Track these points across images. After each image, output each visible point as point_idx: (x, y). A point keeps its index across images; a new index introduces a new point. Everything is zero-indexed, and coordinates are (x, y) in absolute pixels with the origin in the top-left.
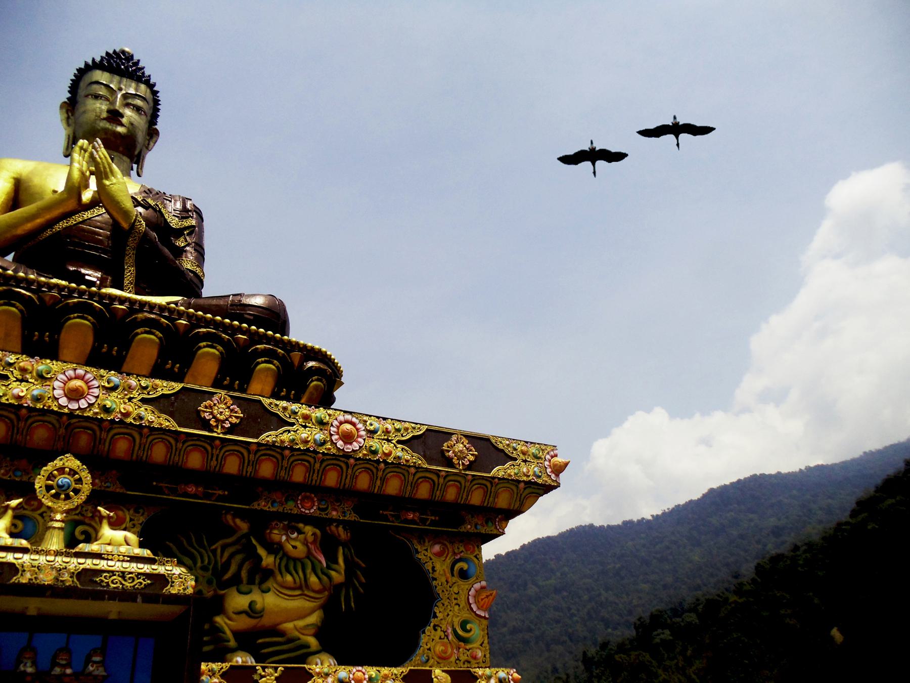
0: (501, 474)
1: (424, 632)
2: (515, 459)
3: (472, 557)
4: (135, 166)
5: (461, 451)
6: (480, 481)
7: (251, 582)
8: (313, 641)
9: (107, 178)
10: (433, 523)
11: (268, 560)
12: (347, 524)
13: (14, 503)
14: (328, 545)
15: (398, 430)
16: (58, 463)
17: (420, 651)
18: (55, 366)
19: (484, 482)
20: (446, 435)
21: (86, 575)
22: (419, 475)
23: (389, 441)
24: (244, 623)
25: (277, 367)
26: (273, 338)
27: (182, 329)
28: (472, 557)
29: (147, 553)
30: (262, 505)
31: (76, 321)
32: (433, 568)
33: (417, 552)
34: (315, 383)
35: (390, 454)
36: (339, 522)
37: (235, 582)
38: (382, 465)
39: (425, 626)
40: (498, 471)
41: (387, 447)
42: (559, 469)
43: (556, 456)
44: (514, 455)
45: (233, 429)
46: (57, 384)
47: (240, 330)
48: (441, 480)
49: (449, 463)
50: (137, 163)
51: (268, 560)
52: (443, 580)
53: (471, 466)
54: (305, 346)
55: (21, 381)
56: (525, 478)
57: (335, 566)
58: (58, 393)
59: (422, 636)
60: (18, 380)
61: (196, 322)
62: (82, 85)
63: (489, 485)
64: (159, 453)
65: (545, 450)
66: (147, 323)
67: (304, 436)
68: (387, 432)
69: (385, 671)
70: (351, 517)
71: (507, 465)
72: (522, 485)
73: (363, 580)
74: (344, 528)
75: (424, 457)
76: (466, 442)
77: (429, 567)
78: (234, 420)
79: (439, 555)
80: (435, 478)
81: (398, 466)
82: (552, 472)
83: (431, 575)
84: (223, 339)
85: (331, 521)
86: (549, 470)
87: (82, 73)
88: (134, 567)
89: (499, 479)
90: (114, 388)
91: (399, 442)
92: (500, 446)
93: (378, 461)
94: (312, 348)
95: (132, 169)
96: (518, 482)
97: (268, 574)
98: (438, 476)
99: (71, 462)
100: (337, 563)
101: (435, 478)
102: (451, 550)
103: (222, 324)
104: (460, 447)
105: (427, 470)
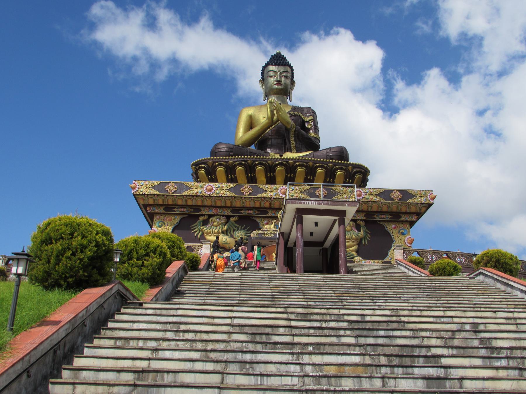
0: (411, 201)
1: (390, 251)
2: (417, 196)
3: (406, 228)
4: (288, 97)
5: (397, 196)
6: (404, 204)
8: (355, 253)
9: (280, 112)
10: (390, 218)
12: (363, 220)
13: (274, 221)
14: (358, 228)
15: (375, 191)
17: (388, 257)
18: (278, 186)
19: (405, 204)
20: (391, 191)
22: (382, 204)
23: (372, 195)
25: (344, 173)
26: (341, 163)
27: (311, 166)
28: (406, 228)
32: (392, 232)
33: (387, 227)
34: (357, 176)
35: (372, 198)
36: (361, 220)
38: (370, 202)
39: (390, 249)
40: (410, 201)
41: (371, 197)
42: (433, 198)
43: (432, 194)
44: (416, 195)
46: (279, 191)
48: (390, 205)
49: (392, 199)
50: (289, 96)
52: (396, 235)
53: (400, 200)
54: (353, 164)
55: (270, 191)
56: (420, 202)
57: (360, 233)
58: (279, 193)
59: (389, 252)
60: (269, 191)
61: (315, 162)
62: (265, 72)
63: (407, 205)
65: (426, 193)
66: (299, 165)
67: (345, 196)
68: (371, 192)
69: (376, 261)
71: (413, 199)
72: (419, 204)
73: (370, 236)
74: (362, 221)
75: (384, 198)
76: (398, 192)
77: (390, 232)
78: (325, 194)
79: (395, 228)
80: (388, 204)
81: (375, 202)
82: (430, 199)
83: (392, 235)
84: (324, 166)
85: (358, 220)
86: (429, 199)
87: (264, 68)
89: (411, 203)
90: (293, 190)
91: (375, 195)
92: (411, 193)
93: (369, 201)
94: (356, 164)
95: (288, 99)
96: (418, 203)
98: (389, 204)
100: (360, 231)
101: (388, 204)
102: (398, 226)
104: (396, 194)
105: (385, 202)
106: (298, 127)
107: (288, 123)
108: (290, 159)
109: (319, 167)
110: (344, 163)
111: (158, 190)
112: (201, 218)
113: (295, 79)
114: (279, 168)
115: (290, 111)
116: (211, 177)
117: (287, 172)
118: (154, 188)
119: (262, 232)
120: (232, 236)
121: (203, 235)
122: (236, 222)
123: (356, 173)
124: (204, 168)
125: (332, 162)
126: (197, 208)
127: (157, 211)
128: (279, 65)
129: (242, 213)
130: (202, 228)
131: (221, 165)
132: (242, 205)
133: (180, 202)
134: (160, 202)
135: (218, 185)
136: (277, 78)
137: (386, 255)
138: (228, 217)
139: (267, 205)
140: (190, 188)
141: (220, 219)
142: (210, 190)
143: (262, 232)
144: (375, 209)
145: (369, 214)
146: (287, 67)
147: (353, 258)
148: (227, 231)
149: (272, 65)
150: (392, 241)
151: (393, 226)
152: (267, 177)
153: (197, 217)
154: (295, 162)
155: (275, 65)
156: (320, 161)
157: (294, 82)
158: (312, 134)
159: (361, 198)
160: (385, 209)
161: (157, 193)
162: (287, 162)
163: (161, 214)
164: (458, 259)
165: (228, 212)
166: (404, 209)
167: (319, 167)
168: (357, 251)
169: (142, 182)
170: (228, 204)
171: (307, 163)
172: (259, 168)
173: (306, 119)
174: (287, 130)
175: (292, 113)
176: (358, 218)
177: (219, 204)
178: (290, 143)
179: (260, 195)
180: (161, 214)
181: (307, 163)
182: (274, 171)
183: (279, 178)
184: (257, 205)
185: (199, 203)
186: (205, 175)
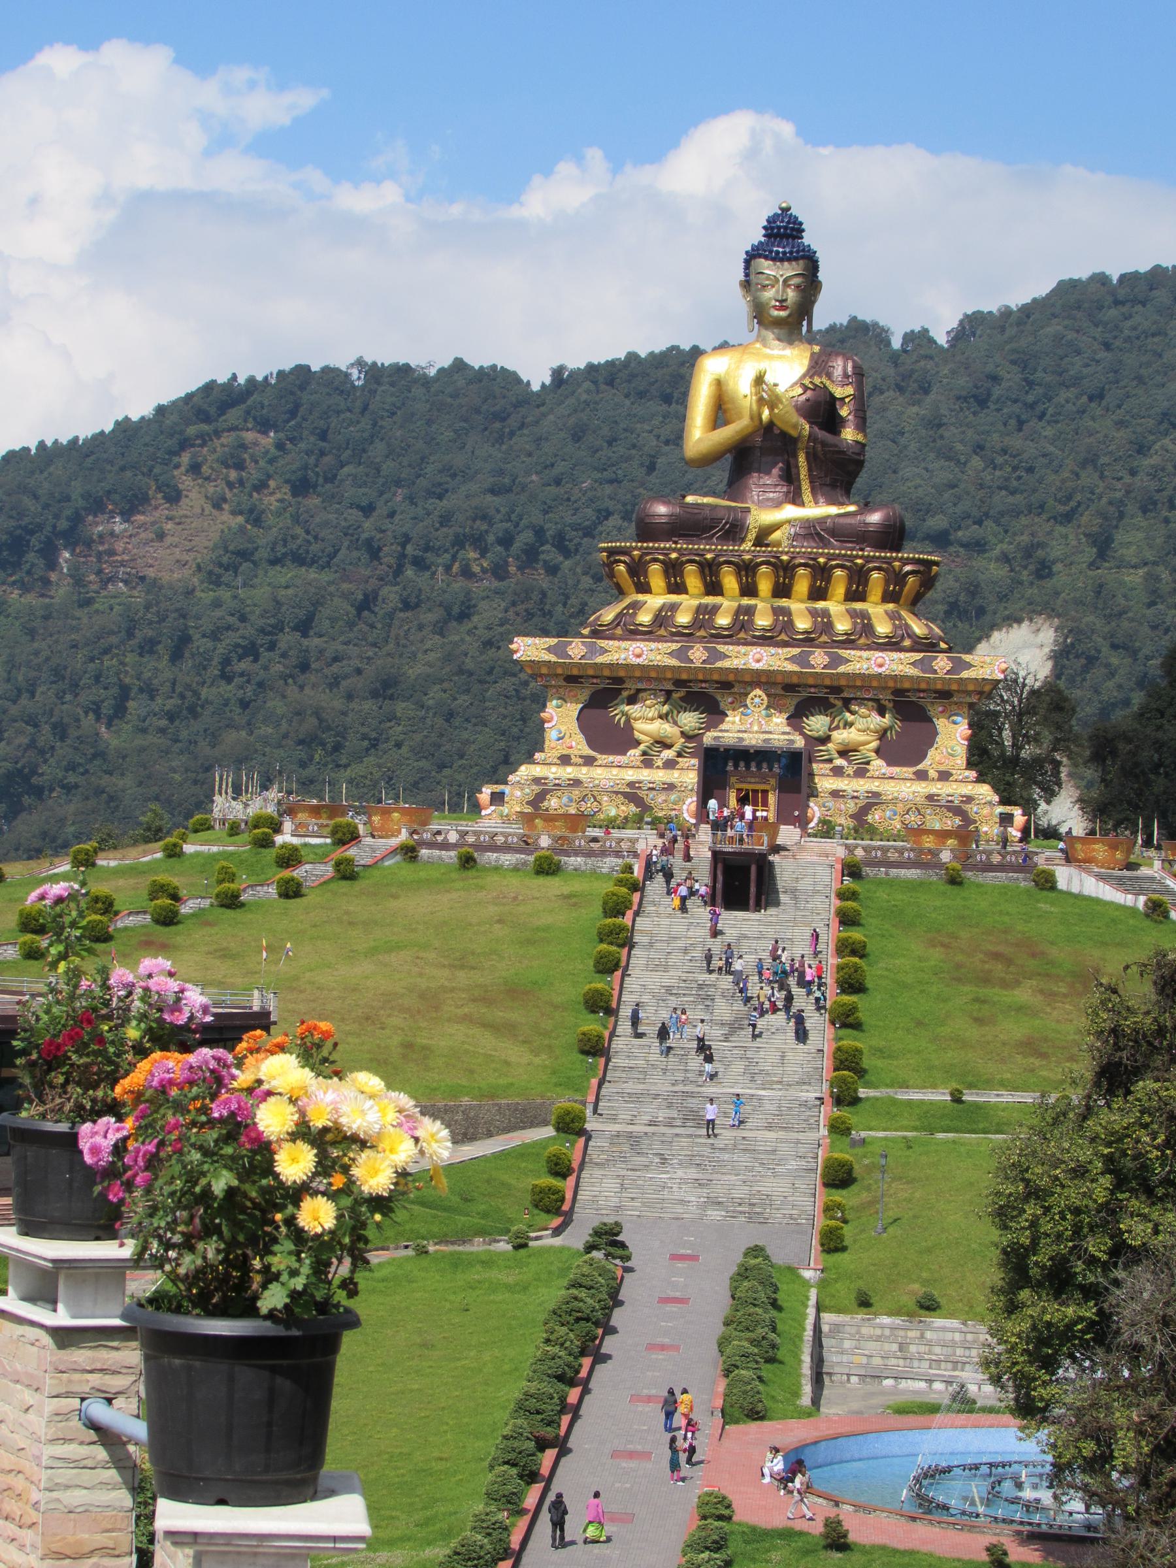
7: (844, 728)
8: (873, 754)
16: (754, 693)
21: (765, 741)
24: (841, 748)
29: (788, 729)
30: (845, 695)
37: (837, 728)
40: (965, 674)
41: (901, 667)
45: (825, 667)
47: (857, 557)
49: (935, 672)
53: (948, 672)
64: (795, 680)
69: (905, 769)
70: (892, 697)
88: (782, 737)
97: (851, 725)
99: (758, 692)
103: (845, 555)
104: (942, 663)
106: (816, 429)
107: (795, 426)
108: (782, 553)
109: (837, 566)
110: (885, 558)
111: (556, 654)
112: (625, 694)
113: (821, 276)
114: (763, 569)
115: (804, 376)
116: (639, 579)
117: (777, 576)
118: (549, 649)
119: (720, 734)
120: (675, 723)
121: (628, 721)
122: (681, 699)
123: (909, 573)
124: (624, 562)
125: (861, 557)
126: (619, 680)
128: (782, 260)
129: (690, 687)
130: (627, 708)
131: (655, 560)
132: (692, 677)
133: (591, 672)
134: (559, 671)
135: (653, 645)
136: (777, 291)
137: (925, 756)
140: (607, 651)
141: (655, 695)
142: (639, 656)
143: (720, 734)
144: (907, 685)
145: (898, 692)
146: (801, 262)
147: (868, 763)
148: (667, 715)
149: (766, 258)
150: (936, 733)
151: (940, 709)
152: (740, 582)
153: (619, 691)
154: (793, 558)
155: (773, 260)
156: (839, 555)
157: (820, 282)
158: (849, 434)
159: (883, 669)
160: (923, 686)
161: (553, 658)
162: (778, 558)
163: (560, 687)
164: (906, 855)
165: (670, 687)
166: (954, 687)
167: (837, 566)
168: (877, 751)
169: (529, 640)
170: (669, 675)
171: (814, 559)
172: (726, 569)
173: (838, 392)
175: (807, 382)
177: (653, 674)
178: (797, 467)
179: (719, 664)
180: (560, 687)
181: (814, 559)
182: (754, 574)
183: (765, 586)
184: (716, 677)
185: (622, 674)
186: (626, 575)
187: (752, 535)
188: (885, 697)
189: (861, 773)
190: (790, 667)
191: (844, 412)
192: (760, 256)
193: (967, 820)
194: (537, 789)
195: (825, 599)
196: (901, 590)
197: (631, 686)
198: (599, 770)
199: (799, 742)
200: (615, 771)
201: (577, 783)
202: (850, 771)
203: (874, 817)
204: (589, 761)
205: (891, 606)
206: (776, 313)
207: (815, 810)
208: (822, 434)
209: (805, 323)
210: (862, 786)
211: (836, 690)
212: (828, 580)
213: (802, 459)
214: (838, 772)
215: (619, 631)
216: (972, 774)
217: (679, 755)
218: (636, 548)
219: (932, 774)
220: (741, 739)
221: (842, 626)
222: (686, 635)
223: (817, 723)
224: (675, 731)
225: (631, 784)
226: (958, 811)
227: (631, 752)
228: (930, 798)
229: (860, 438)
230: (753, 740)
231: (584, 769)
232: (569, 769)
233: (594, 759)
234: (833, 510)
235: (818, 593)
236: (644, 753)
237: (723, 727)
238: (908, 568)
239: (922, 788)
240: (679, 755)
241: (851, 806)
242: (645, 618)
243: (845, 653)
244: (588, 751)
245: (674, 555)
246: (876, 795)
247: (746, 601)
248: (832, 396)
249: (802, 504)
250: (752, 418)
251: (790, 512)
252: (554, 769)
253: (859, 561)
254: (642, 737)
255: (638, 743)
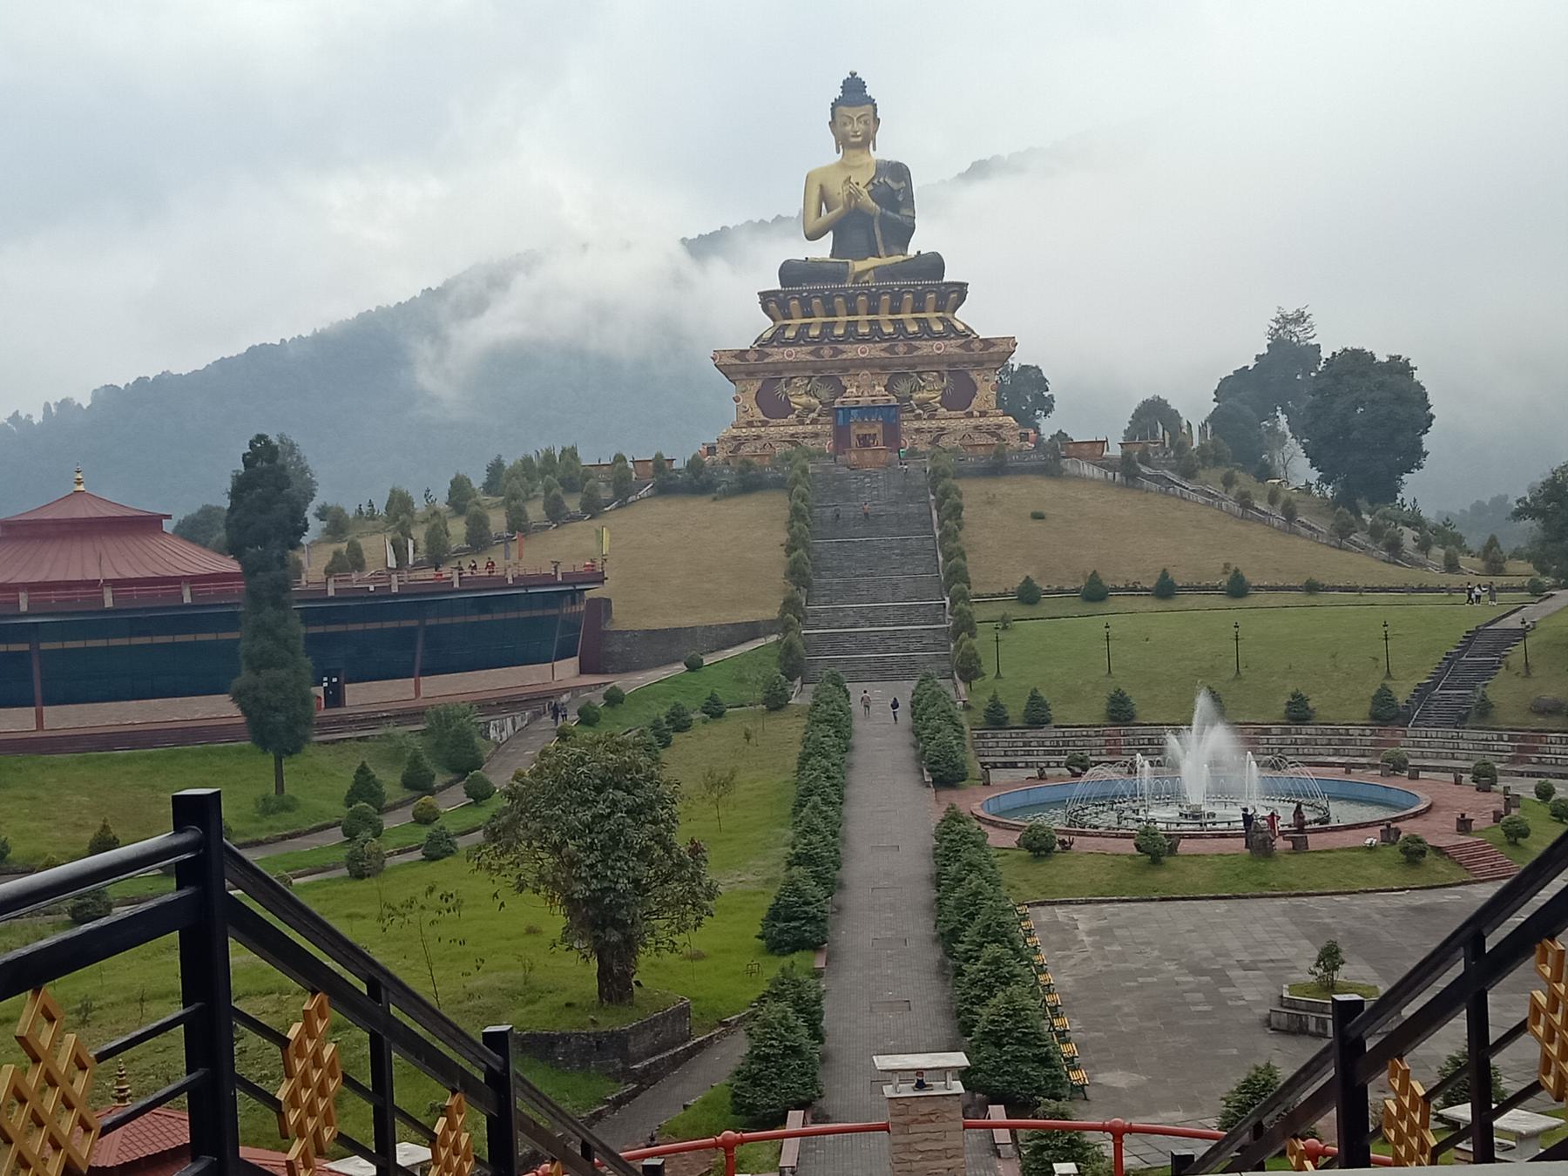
8: (938, 405)
11: (923, 384)
21: (873, 401)
31: (860, 298)
37: (915, 390)
49: (973, 350)
51: (923, 384)
81: (956, 354)
107: (871, 209)
108: (872, 287)
112: (783, 380)
113: (878, 116)
115: (873, 178)
121: (786, 398)
126: (780, 372)
127: (739, 377)
134: (742, 368)
138: (810, 378)
139: (848, 362)
144: (956, 359)
145: (950, 365)
152: (847, 307)
160: (966, 359)
173: (895, 186)
174: (872, 218)
175: (875, 182)
176: (940, 369)
183: (862, 308)
185: (780, 367)
187: (851, 278)
188: (943, 368)
189: (931, 417)
190: (883, 354)
191: (900, 199)
192: (840, 105)
193: (999, 437)
194: (735, 443)
195: (899, 313)
196: (946, 302)
197: (787, 375)
198: (772, 429)
199: (894, 402)
200: (782, 429)
201: (759, 437)
202: (926, 416)
203: (945, 442)
204: (764, 424)
205: (941, 314)
206: (853, 140)
207: (907, 442)
208: (890, 213)
209: (871, 145)
210: (934, 424)
211: (912, 366)
212: (901, 300)
213: (877, 231)
214: (918, 417)
215: (775, 344)
216: (1000, 411)
217: (819, 415)
218: (781, 291)
219: (975, 413)
220: (858, 402)
221: (912, 328)
222: (817, 342)
223: (903, 387)
224: (816, 401)
225: (792, 436)
226: (993, 434)
227: (790, 417)
228: (976, 428)
229: (911, 214)
230: (865, 401)
231: (763, 429)
232: (753, 430)
233: (768, 422)
234: (901, 258)
235: (894, 310)
236: (798, 416)
237: (846, 395)
238: (951, 290)
239: (973, 422)
240: (819, 415)
241: (928, 437)
242: (790, 334)
243: (917, 343)
244: (763, 418)
245: (805, 294)
246: (944, 429)
247: (850, 318)
248: (892, 189)
249: (880, 257)
250: (845, 206)
251: (872, 262)
252: (744, 430)
253: (920, 288)
254: (797, 406)
255: (795, 410)
